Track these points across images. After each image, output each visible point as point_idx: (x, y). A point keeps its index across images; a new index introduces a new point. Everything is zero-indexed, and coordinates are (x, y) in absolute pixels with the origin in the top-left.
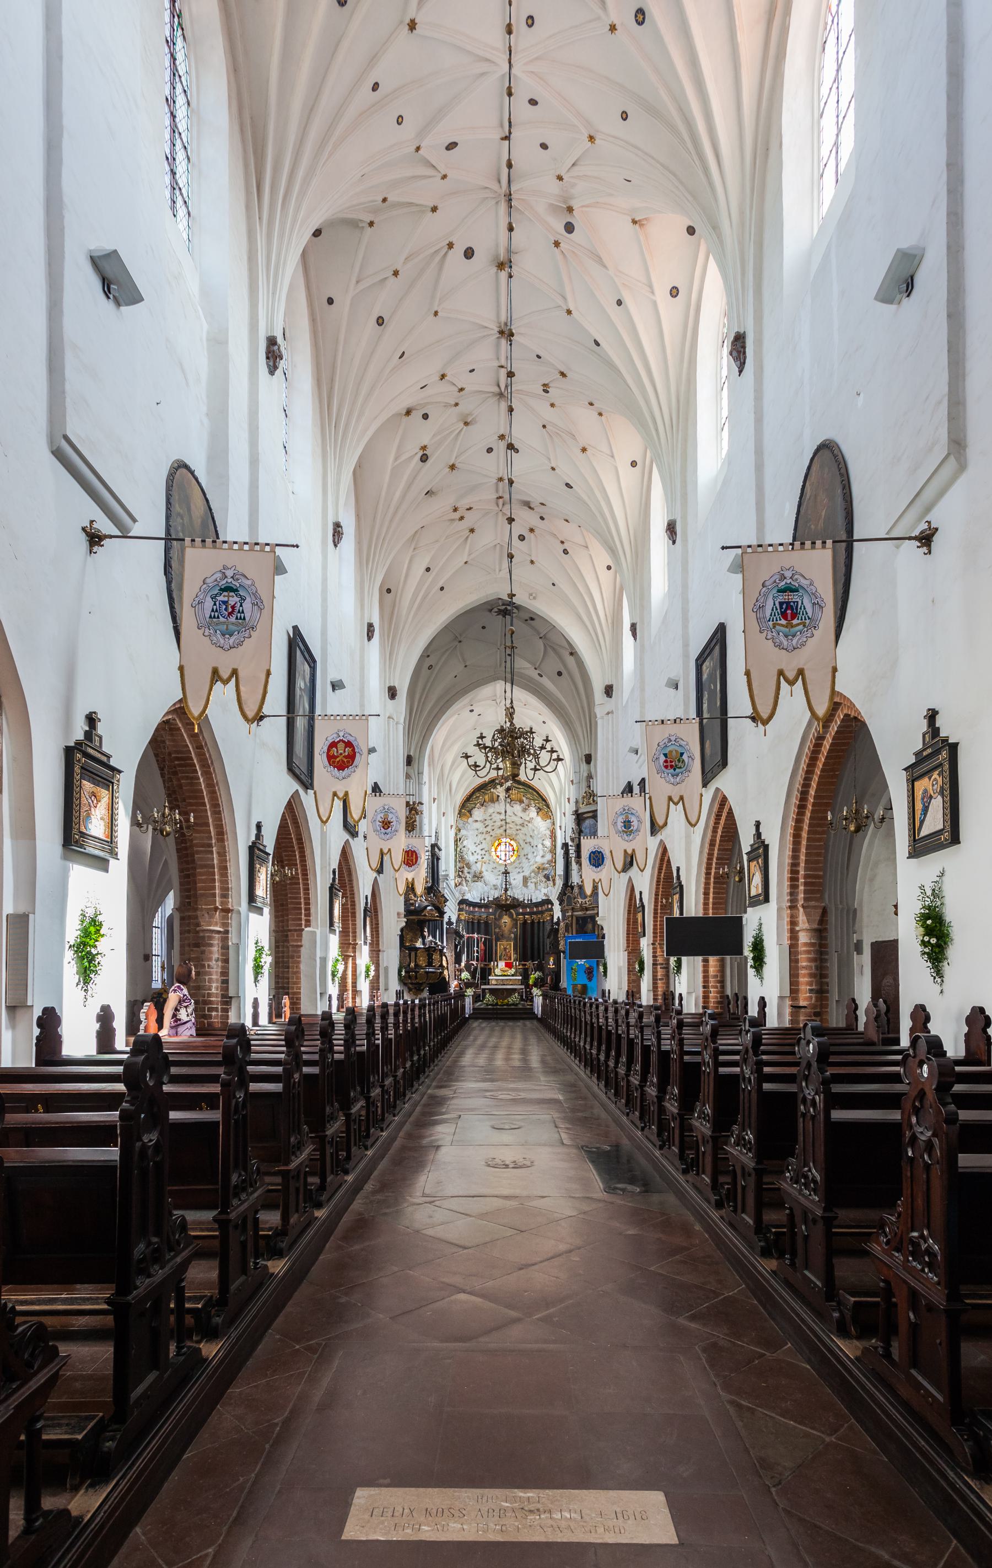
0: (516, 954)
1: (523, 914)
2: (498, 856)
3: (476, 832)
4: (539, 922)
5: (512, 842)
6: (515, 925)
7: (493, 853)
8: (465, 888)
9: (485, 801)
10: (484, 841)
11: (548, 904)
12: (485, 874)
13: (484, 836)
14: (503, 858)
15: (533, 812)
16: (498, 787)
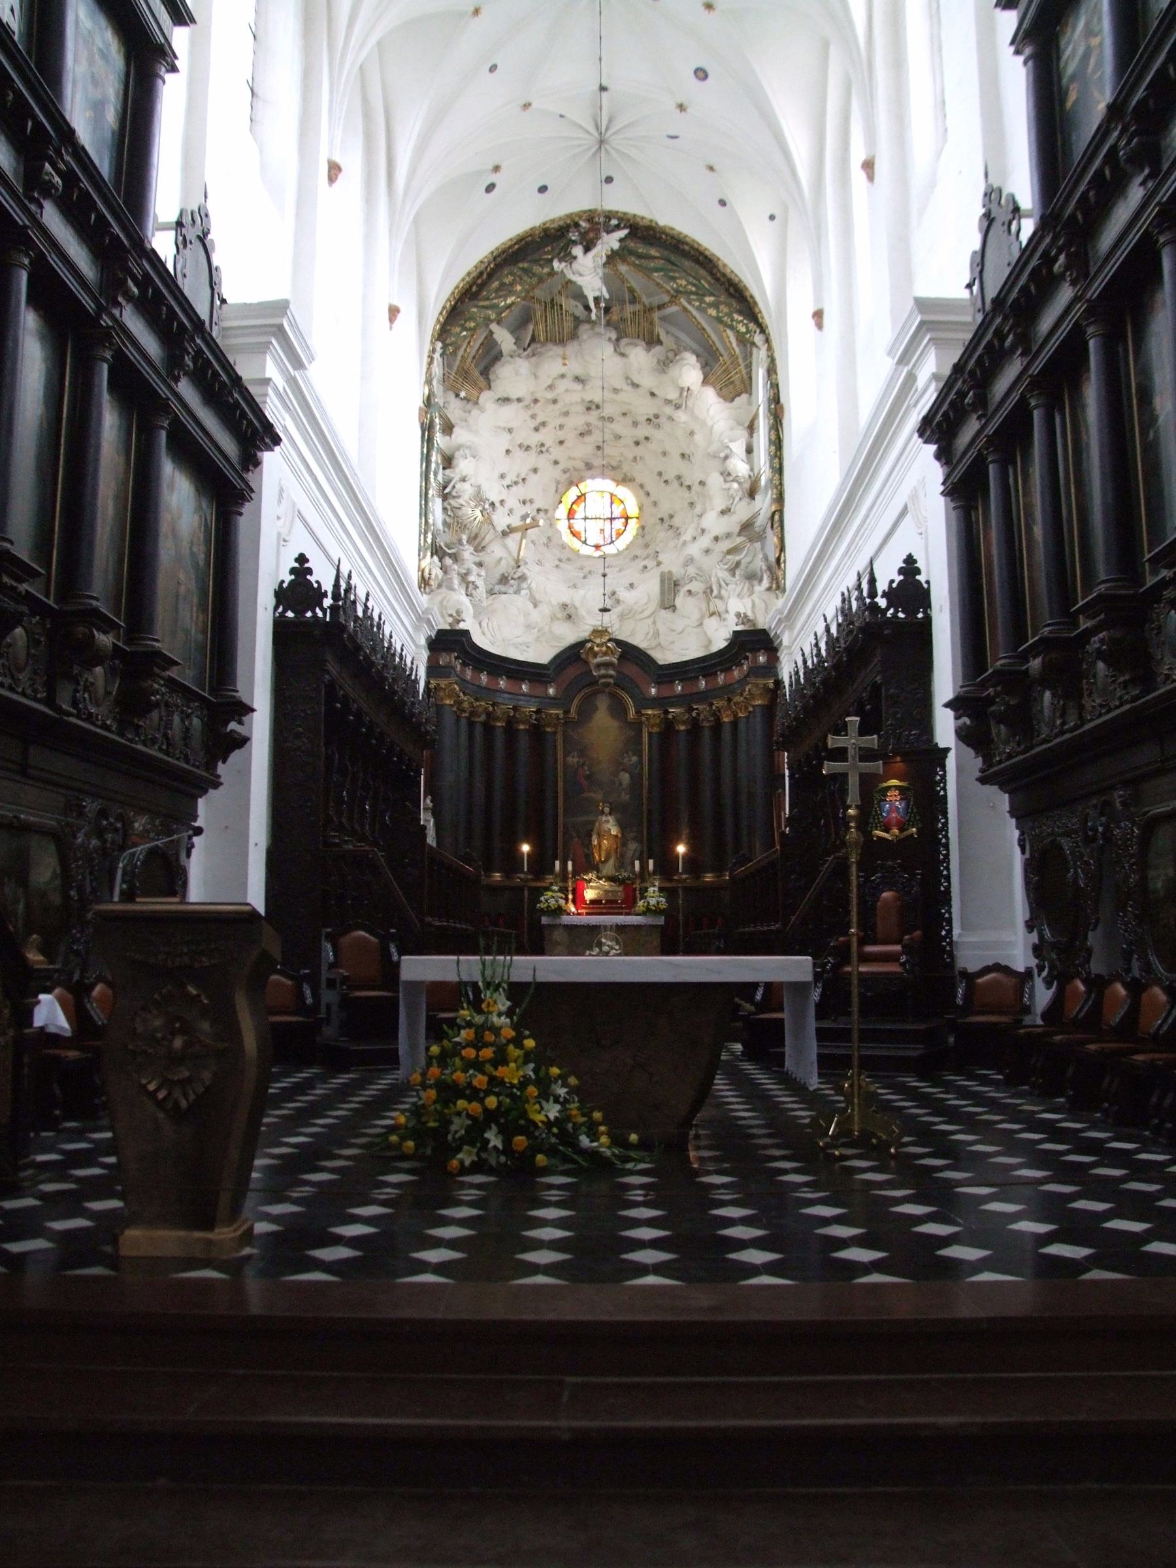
0: (641, 842)
1: (661, 702)
2: (575, 534)
3: (504, 441)
4: (717, 726)
5: (623, 492)
6: (634, 744)
7: (562, 526)
8: (459, 597)
9: (533, 339)
10: (533, 479)
11: (755, 651)
12: (531, 571)
13: (532, 459)
14: (594, 538)
15: (690, 373)
16: (577, 251)
